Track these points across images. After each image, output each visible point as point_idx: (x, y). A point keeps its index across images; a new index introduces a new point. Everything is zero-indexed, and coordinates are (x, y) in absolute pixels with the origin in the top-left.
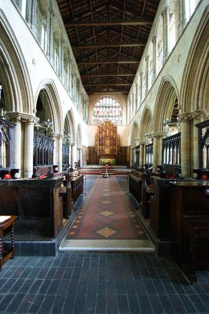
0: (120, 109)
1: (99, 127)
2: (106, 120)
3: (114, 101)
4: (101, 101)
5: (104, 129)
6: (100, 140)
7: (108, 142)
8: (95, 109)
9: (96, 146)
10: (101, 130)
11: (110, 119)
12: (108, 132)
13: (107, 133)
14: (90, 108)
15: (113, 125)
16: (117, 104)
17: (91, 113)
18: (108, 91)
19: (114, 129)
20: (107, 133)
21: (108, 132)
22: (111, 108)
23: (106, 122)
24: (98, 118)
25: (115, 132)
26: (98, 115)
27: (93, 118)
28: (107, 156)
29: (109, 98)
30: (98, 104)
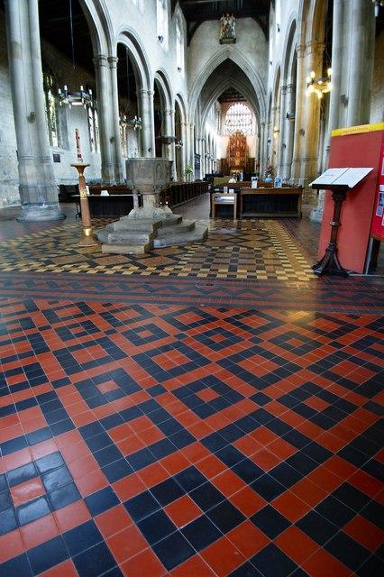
3: (245, 107)
6: (231, 151)
7: (238, 154)
9: (228, 157)
10: (232, 141)
11: (240, 128)
13: (238, 144)
16: (248, 111)
17: (223, 123)
18: (239, 101)
19: (244, 140)
20: (238, 144)
24: (229, 128)
25: (245, 143)
27: (225, 128)
28: (237, 168)
30: (229, 112)
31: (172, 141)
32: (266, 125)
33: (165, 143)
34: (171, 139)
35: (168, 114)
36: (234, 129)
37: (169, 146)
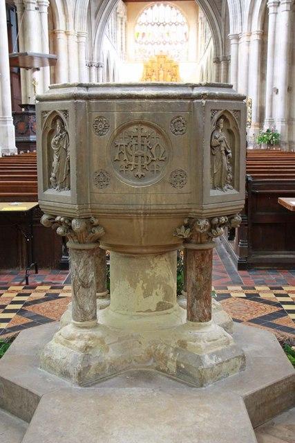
0: (186, 26)
1: (147, 67)
2: (158, 53)
3: (174, 11)
4: (149, 11)
5: (156, 69)
8: (139, 29)
11: (165, 49)
12: (161, 76)
14: (129, 25)
15: (170, 62)
16: (181, 18)
21: (161, 76)
22: (167, 26)
23: (158, 57)
26: (144, 40)
29: (165, 5)
30: (142, 18)
31: (43, 65)
32: (244, 39)
33: (27, 68)
34: (41, 58)
35: (33, 7)
36: (157, 50)
37: (37, 75)
